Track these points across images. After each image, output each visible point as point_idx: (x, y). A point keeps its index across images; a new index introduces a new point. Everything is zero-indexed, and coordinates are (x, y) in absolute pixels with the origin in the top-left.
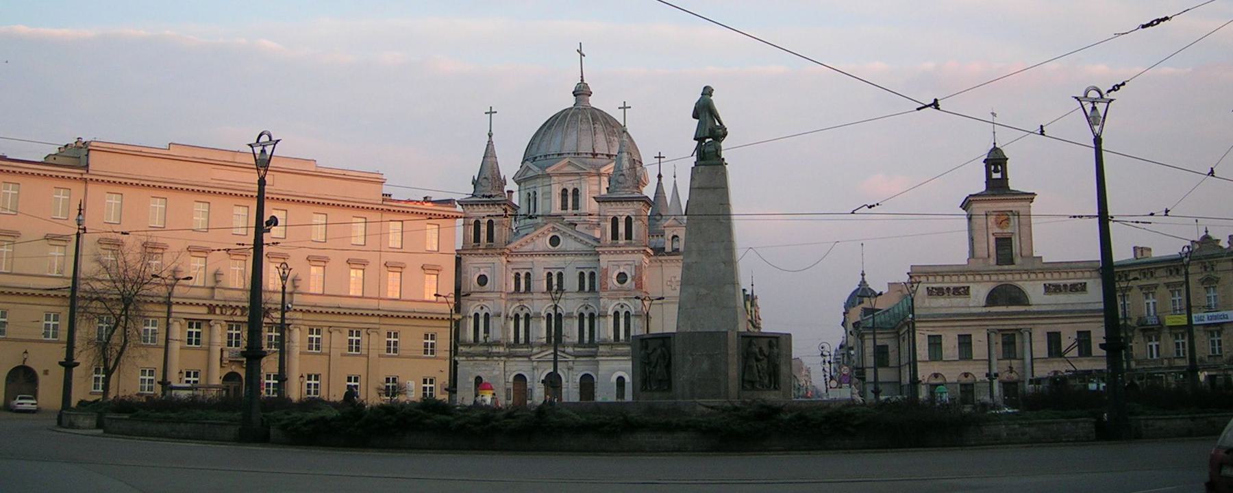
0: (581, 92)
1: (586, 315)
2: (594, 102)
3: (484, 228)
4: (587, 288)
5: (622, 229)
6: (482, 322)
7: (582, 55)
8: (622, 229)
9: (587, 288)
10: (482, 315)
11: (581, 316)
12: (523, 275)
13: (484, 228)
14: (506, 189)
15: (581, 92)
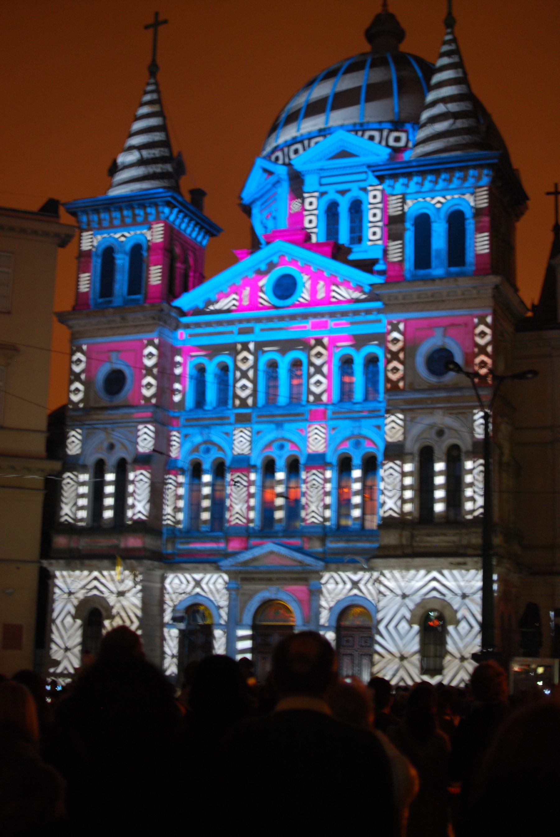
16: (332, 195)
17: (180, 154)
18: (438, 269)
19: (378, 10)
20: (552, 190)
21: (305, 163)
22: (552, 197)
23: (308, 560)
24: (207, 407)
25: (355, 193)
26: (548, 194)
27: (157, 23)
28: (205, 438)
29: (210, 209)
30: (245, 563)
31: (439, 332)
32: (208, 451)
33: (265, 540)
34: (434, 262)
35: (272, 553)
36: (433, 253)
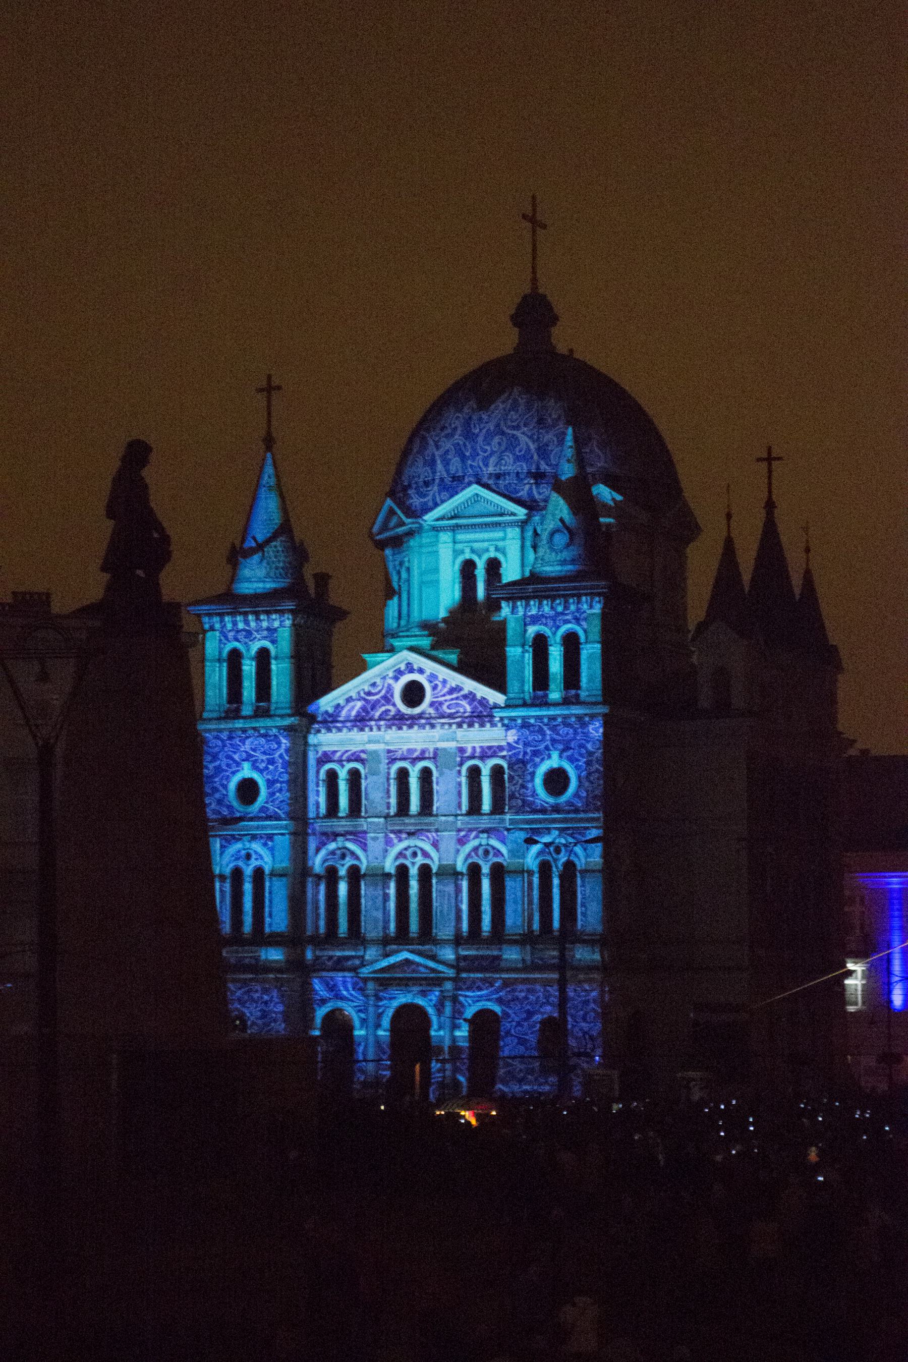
0: (535, 314)
1: (485, 869)
2: (563, 338)
3: (249, 668)
4: (486, 806)
5: (556, 665)
6: (248, 887)
7: (532, 219)
8: (556, 665)
9: (486, 806)
10: (248, 871)
11: (474, 872)
12: (343, 774)
13: (249, 668)
14: (308, 572)
15: (535, 314)
16: (468, 555)
17: (302, 543)
18: (555, 695)
19: (527, 289)
20: (765, 455)
21: (437, 520)
22: (764, 465)
23: (441, 968)
24: (340, 815)
25: (492, 554)
26: (759, 460)
27: (269, 389)
28: (340, 845)
29: (337, 597)
30: (383, 970)
31: (555, 755)
32: (343, 856)
33: (401, 947)
34: (552, 686)
35: (407, 962)
36: (551, 677)
